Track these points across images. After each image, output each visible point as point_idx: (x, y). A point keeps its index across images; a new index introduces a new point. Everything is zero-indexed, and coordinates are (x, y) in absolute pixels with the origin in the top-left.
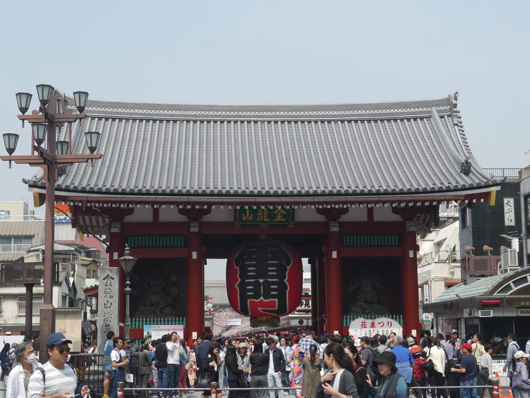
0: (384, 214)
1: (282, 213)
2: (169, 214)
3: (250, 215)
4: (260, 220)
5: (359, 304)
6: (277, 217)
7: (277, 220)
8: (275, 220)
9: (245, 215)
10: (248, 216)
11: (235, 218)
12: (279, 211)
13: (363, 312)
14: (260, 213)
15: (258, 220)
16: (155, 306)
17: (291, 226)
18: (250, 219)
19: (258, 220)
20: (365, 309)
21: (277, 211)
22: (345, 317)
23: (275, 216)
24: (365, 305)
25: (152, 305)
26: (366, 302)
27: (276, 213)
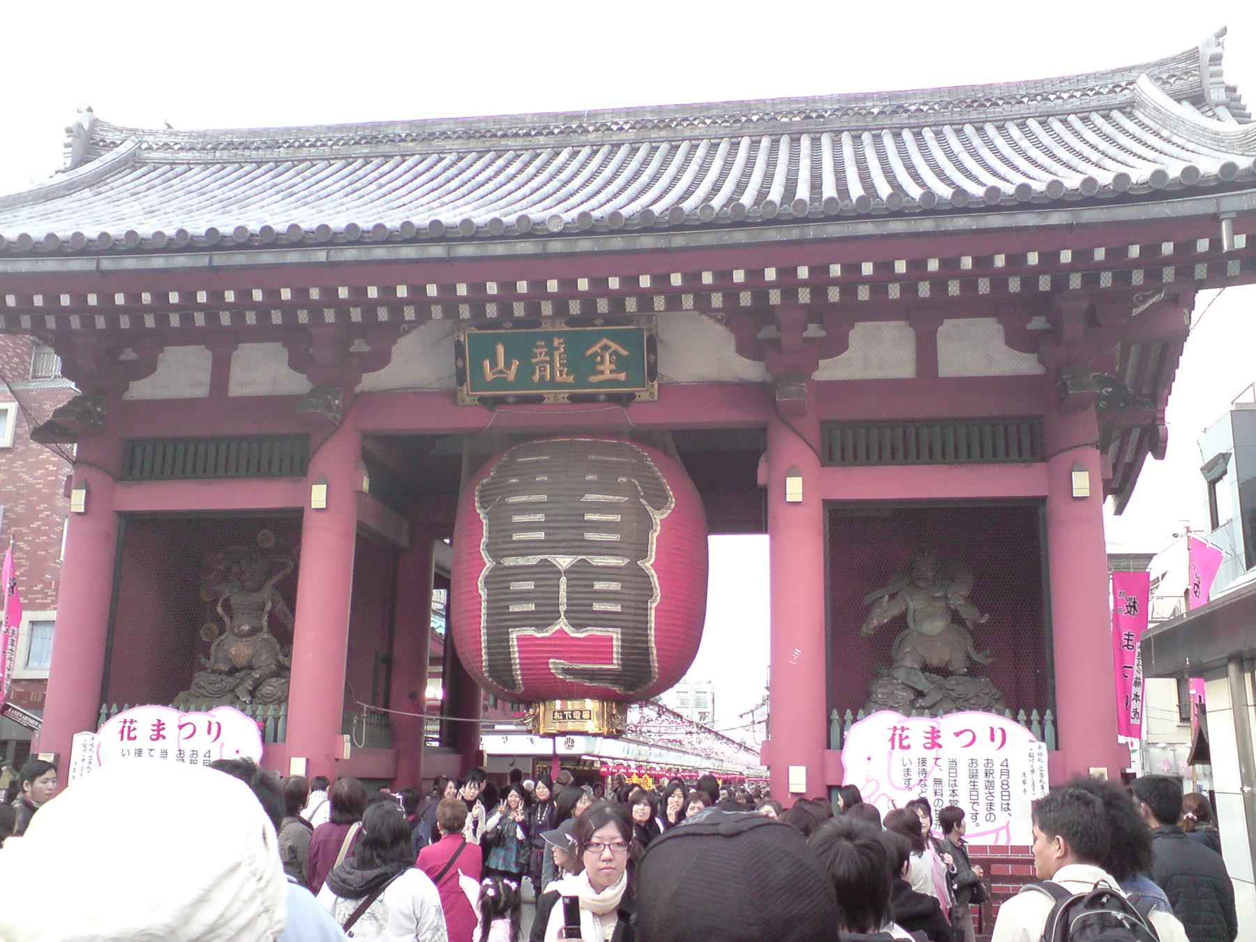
0: (976, 351)
1: (615, 353)
2: (262, 372)
3: (508, 365)
4: (542, 377)
5: (900, 674)
6: (600, 368)
7: (601, 377)
8: (593, 379)
9: (494, 364)
10: (501, 365)
11: (461, 377)
12: (606, 348)
13: (912, 703)
14: (541, 355)
15: (536, 378)
16: (243, 673)
17: (645, 396)
18: (511, 375)
19: (536, 378)
20: (920, 694)
21: (596, 348)
22: (835, 715)
23: (591, 365)
24: (922, 682)
25: (233, 671)
26: (925, 668)
27: (596, 354)
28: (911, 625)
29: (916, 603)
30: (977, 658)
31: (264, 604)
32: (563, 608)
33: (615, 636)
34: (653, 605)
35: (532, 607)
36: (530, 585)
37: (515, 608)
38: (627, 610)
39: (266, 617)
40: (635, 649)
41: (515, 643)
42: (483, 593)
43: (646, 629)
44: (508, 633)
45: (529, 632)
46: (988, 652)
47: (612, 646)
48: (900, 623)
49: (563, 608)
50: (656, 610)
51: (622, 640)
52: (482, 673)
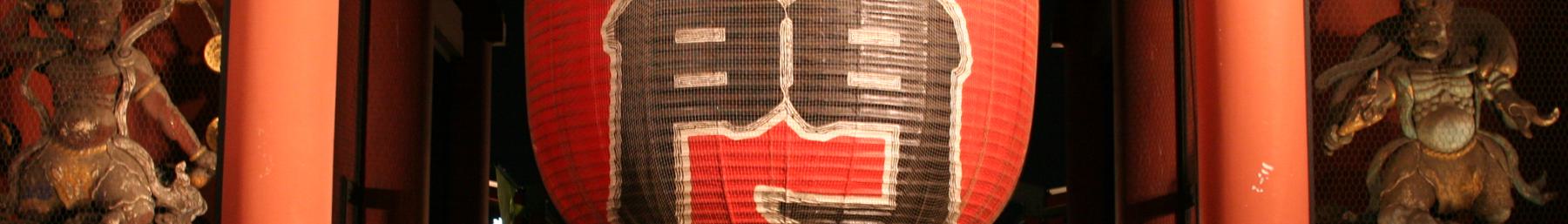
28: (1409, 131)
29: (1421, 90)
30: (1527, 191)
31: (121, 78)
32: (786, 82)
33: (888, 139)
34: (960, 78)
35: (720, 79)
36: (718, 36)
37: (686, 81)
38: (914, 89)
39: (125, 104)
40: (925, 166)
41: (686, 151)
42: (613, 52)
43: (947, 127)
44: (672, 133)
45: (722, 130)
46: (1543, 180)
47: (881, 161)
48: (1387, 130)
49: (786, 82)
50: (966, 90)
51: (903, 149)
52: (604, 214)
